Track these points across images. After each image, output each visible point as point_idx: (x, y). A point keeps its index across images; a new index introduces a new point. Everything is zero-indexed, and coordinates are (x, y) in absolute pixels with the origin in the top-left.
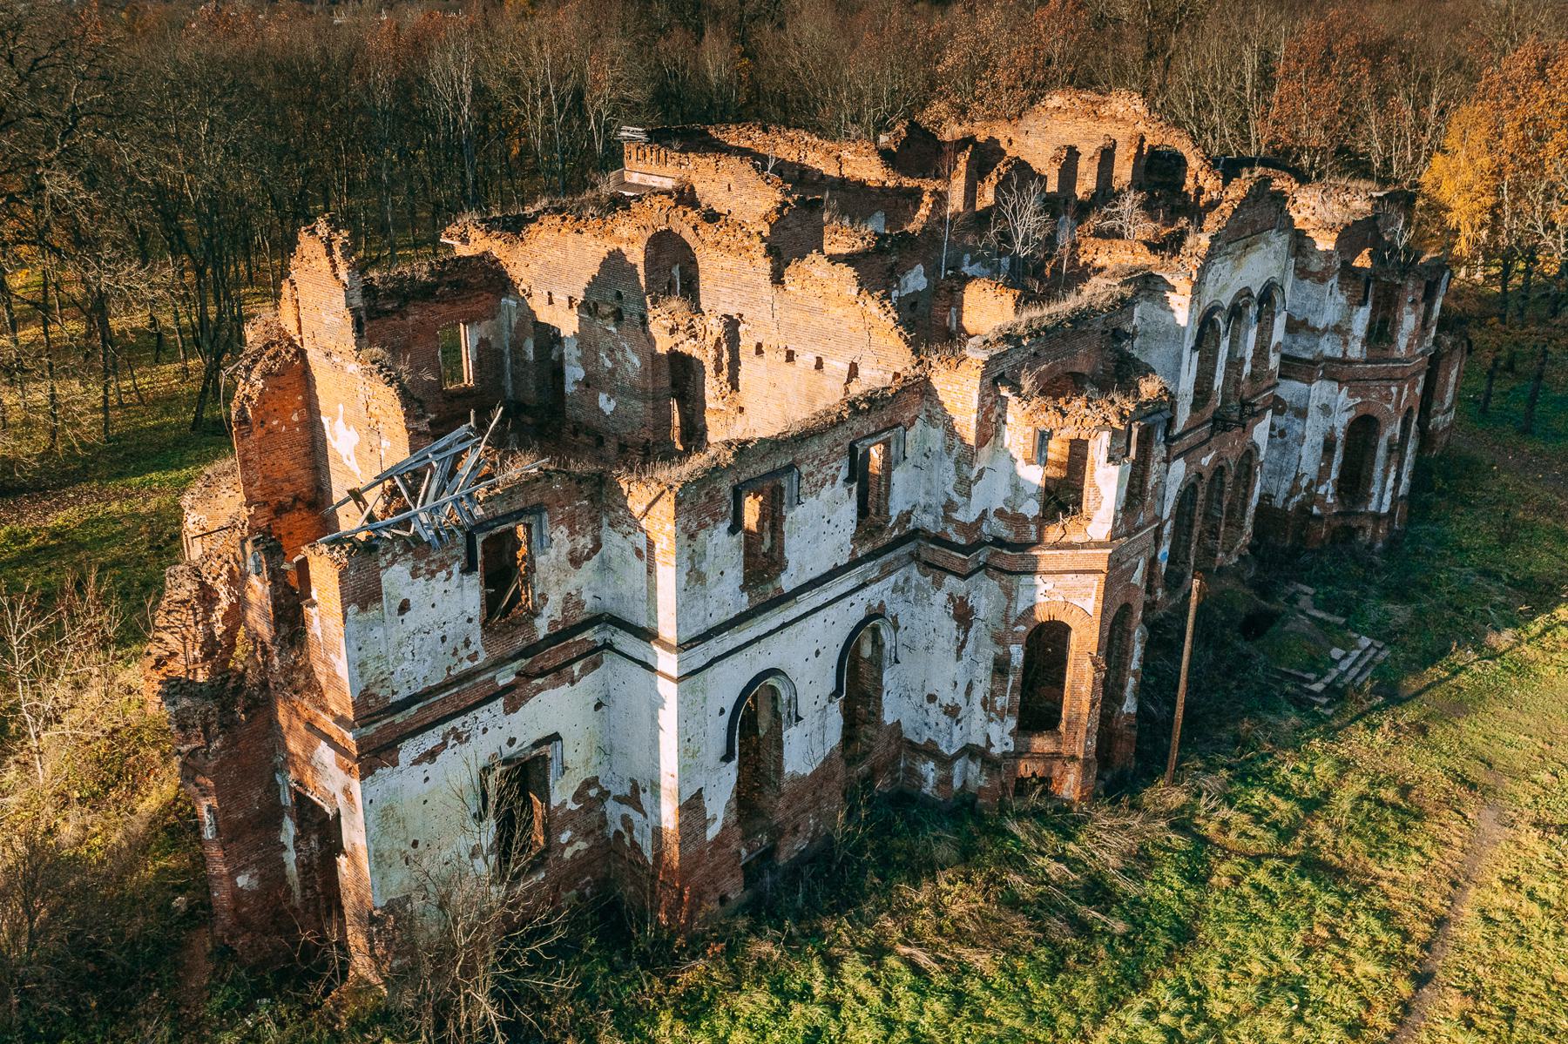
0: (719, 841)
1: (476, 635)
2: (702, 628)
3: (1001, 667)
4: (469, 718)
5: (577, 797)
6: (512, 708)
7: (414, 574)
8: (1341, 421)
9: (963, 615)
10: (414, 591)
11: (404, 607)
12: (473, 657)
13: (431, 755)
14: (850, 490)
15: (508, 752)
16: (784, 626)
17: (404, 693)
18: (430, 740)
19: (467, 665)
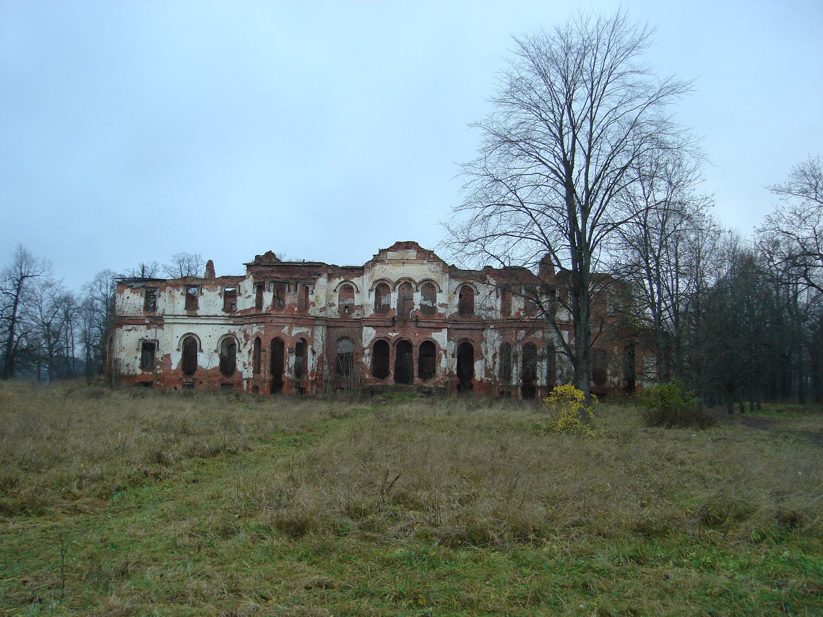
0: (176, 372)
1: (142, 309)
2: (172, 314)
3: (249, 352)
4: (138, 326)
5: (162, 358)
6: (148, 328)
7: (131, 292)
8: (498, 344)
9: (246, 337)
10: (131, 295)
11: (128, 298)
12: (141, 313)
13: (130, 330)
14: (221, 297)
15: (145, 338)
16: (197, 323)
17: (125, 315)
18: (130, 327)
19: (139, 315)
